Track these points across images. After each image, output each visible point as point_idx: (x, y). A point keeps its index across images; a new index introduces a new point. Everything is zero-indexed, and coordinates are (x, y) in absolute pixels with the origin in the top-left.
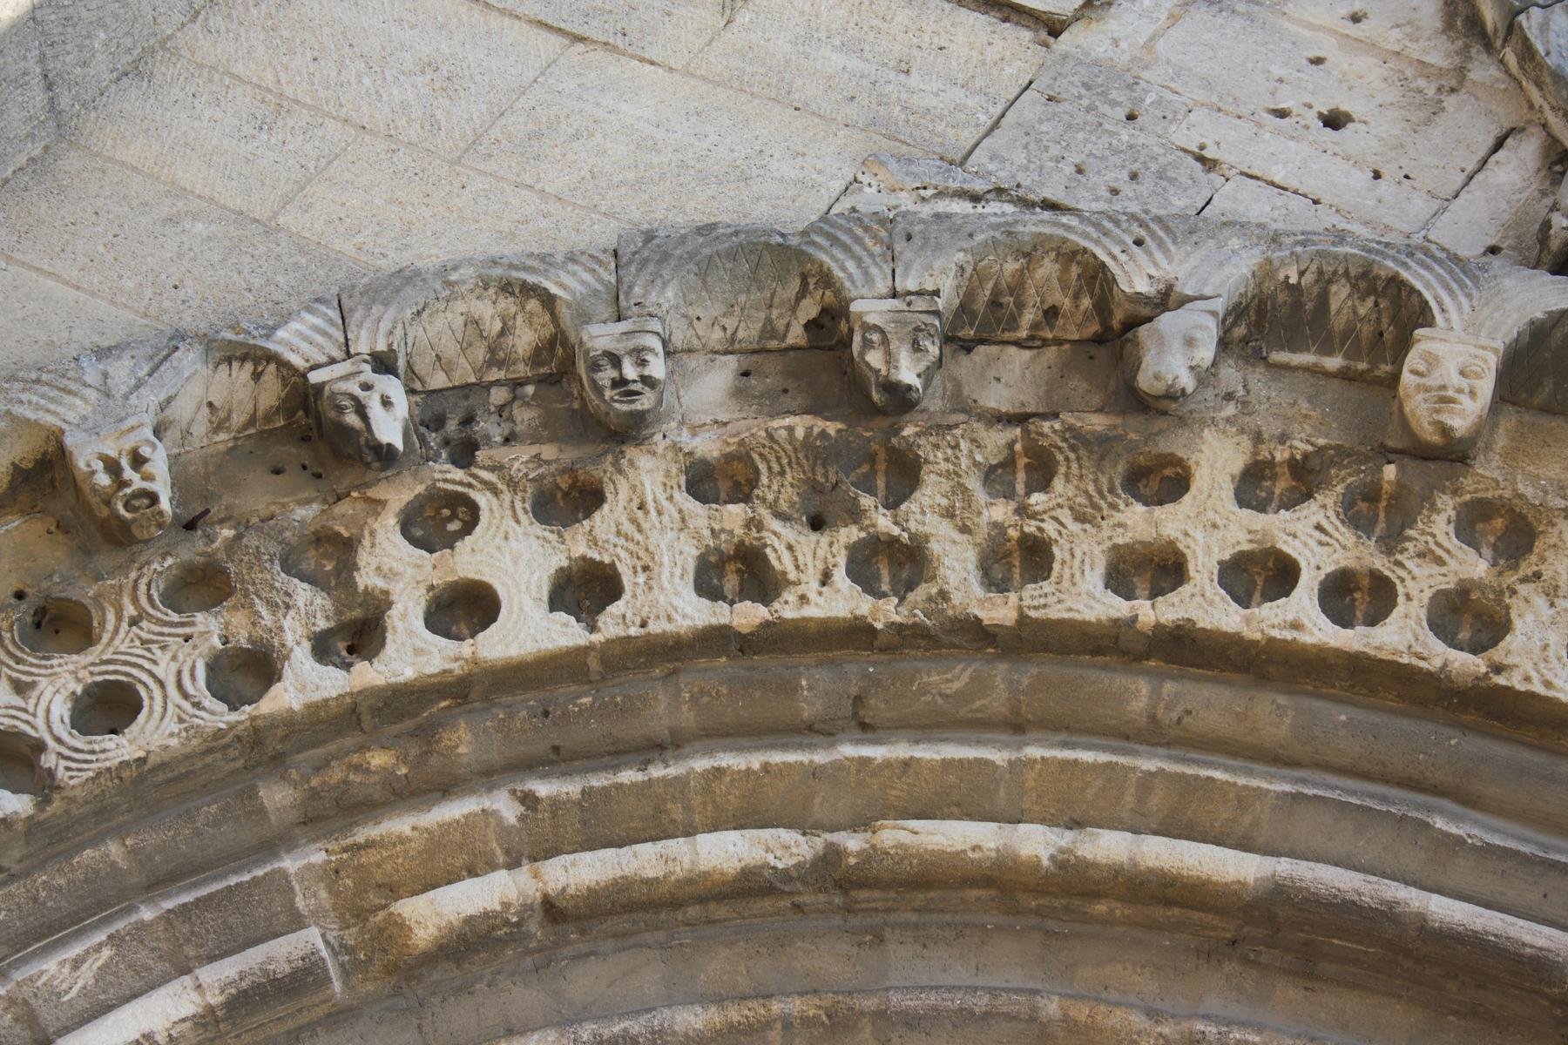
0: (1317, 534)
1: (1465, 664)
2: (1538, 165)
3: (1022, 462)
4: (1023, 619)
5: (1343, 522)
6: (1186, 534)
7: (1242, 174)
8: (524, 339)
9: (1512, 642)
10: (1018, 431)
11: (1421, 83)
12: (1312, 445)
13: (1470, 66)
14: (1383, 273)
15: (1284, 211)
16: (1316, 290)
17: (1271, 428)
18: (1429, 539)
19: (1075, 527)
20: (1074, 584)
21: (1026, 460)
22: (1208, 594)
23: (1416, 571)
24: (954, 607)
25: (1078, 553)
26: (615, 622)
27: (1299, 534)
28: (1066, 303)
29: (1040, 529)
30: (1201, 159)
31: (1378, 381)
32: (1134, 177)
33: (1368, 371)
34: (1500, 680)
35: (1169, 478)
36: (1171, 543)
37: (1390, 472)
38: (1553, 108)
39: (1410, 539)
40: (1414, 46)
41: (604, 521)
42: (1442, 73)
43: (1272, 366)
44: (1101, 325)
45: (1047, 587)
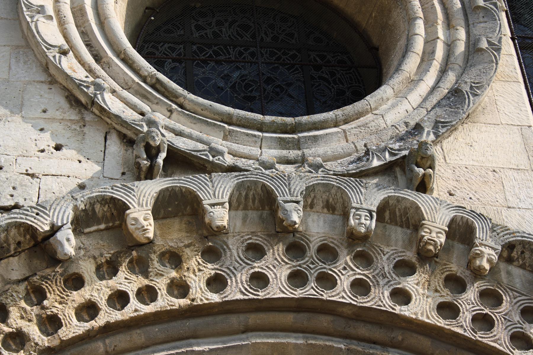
0: (126, 281)
1: (184, 302)
2: (120, 142)
3: (31, 291)
4: (62, 341)
5: (131, 274)
6: (92, 296)
7: (43, 175)
10: (26, 283)
11: (74, 127)
12: (110, 254)
13: (84, 116)
14: (108, 197)
15: (62, 183)
16: (91, 209)
17: (97, 253)
18: (156, 269)
19: (60, 306)
20: (71, 325)
21: (32, 290)
22: (108, 311)
23: (157, 280)
24: (41, 346)
25: (67, 315)
27: (122, 282)
28: (22, 239)
29: (52, 312)
30: (28, 175)
31: (116, 227)
32: (14, 188)
33: (113, 225)
34: (195, 303)
35: (74, 279)
36: (90, 300)
37: (134, 253)
38: (116, 124)
39: (151, 272)
40: (65, 115)
42: (78, 122)
43: (85, 234)
44: (34, 241)
45: (64, 328)
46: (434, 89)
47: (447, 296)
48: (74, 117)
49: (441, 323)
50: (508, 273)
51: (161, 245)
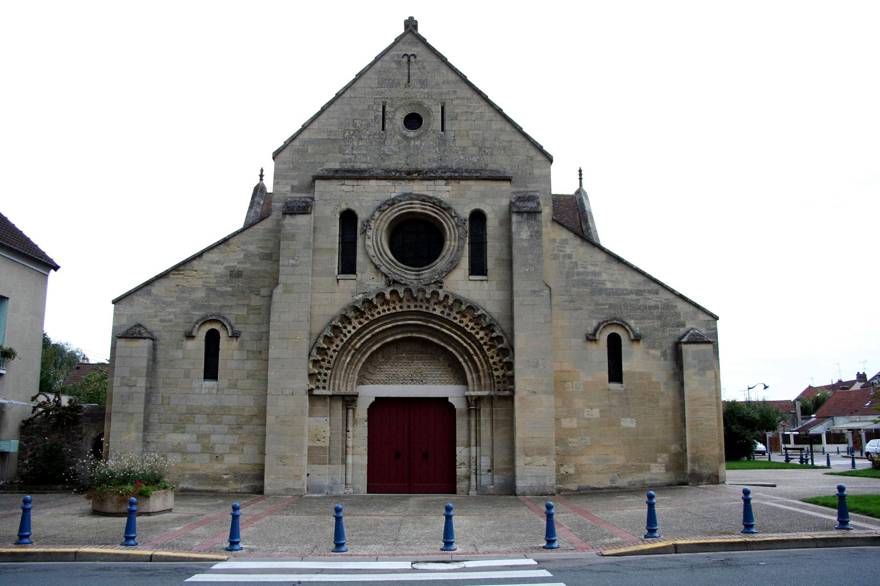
26: (357, 329)
41: (353, 323)
47: (443, 309)
49: (441, 315)
51: (392, 300)
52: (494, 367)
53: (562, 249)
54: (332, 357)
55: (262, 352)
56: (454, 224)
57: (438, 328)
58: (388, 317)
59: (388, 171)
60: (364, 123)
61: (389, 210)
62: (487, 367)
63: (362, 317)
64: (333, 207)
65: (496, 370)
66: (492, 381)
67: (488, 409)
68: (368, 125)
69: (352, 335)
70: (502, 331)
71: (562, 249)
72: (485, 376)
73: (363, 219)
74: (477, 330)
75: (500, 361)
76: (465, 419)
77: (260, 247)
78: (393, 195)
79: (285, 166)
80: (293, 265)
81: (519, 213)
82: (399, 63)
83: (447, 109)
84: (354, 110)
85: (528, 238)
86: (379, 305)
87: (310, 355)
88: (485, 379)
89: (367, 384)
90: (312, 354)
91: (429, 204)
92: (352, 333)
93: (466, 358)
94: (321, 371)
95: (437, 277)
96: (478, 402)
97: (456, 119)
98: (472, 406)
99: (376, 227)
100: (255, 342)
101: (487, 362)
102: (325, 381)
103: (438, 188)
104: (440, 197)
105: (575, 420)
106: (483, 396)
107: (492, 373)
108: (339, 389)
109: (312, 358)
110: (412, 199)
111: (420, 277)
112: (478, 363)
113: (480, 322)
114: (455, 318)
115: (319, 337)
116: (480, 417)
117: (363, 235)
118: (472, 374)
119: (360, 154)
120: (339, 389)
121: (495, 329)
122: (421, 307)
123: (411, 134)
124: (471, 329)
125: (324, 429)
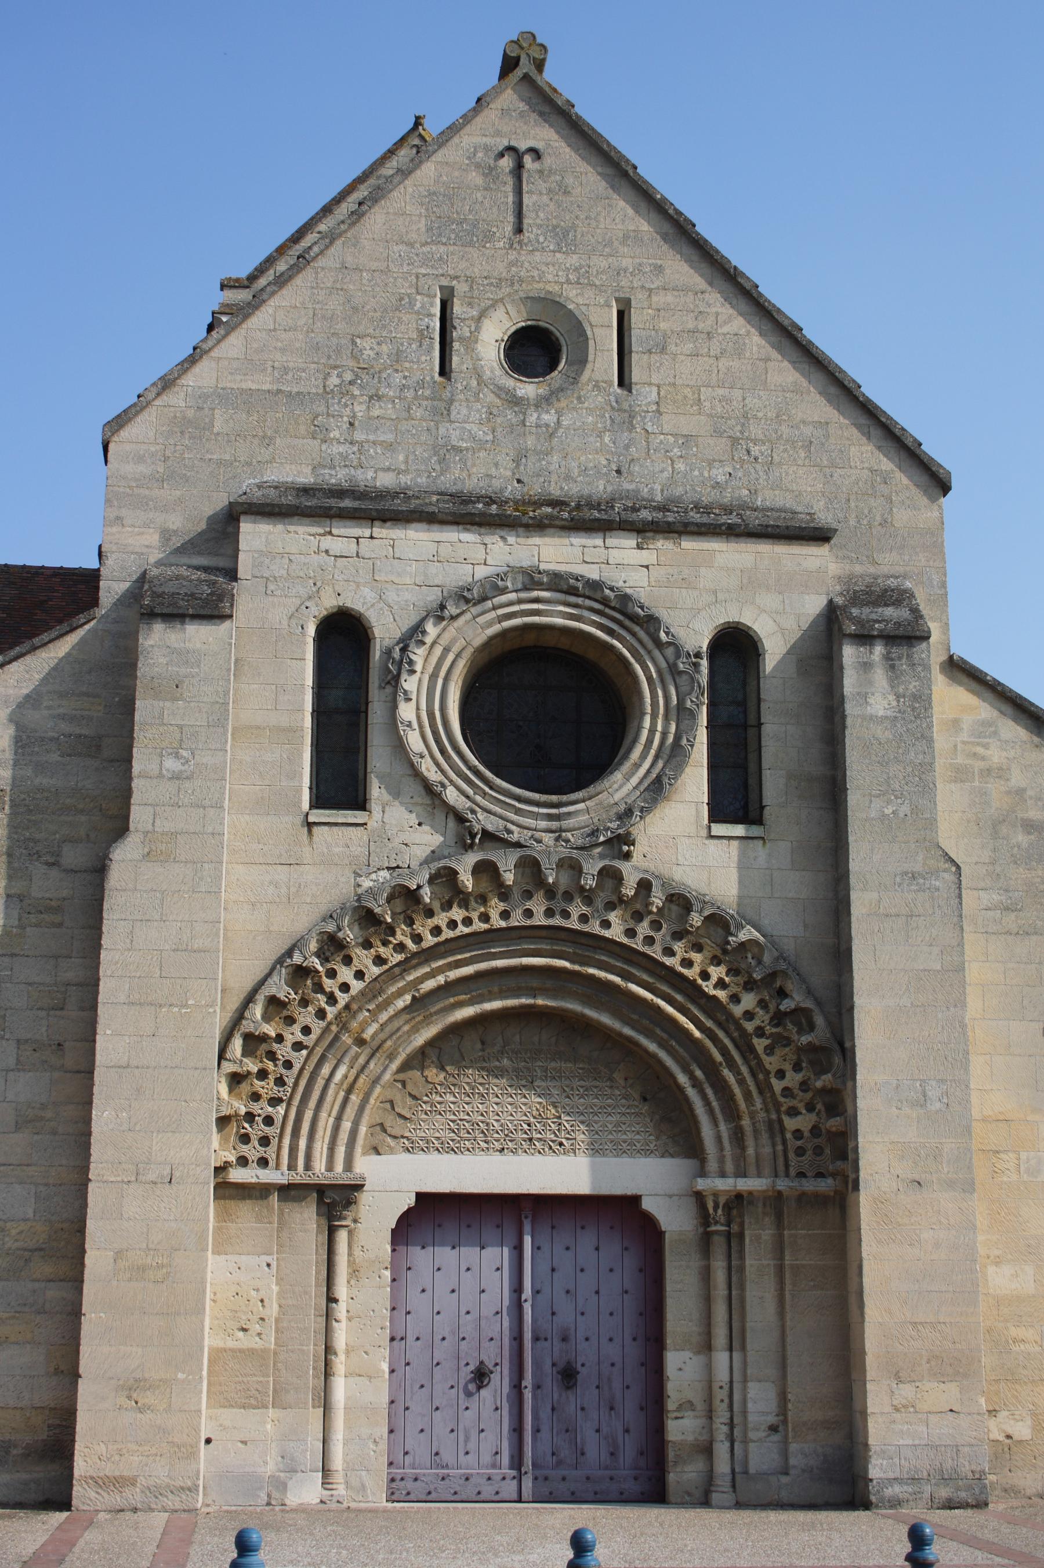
1: (485, 926)
8: (325, 937)
9: (491, 920)
41: (355, 961)
46: (649, 772)
47: (631, 924)
48: (429, 802)
49: (625, 940)
50: (669, 909)
52: (786, 1103)
53: (980, 750)
54: (288, 1065)
55: (67, 1045)
56: (663, 665)
57: (617, 980)
58: (462, 943)
59: (463, 499)
60: (384, 348)
61: (468, 616)
62: (764, 1102)
63: (385, 943)
64: (293, 602)
65: (793, 1112)
66: (780, 1148)
67: (767, 1234)
68: (398, 356)
69: (353, 998)
70: (809, 992)
71: (980, 750)
72: (756, 1131)
73: (387, 642)
74: (734, 989)
75: (804, 1086)
76: (695, 1262)
77: (62, 717)
78: (481, 572)
79: (142, 469)
80: (176, 777)
81: (864, 638)
82: (489, 172)
83: (636, 319)
84: (355, 309)
85: (889, 713)
86: (436, 906)
87: (221, 1057)
88: (756, 1139)
89: (392, 1151)
90: (228, 1055)
91: (588, 603)
92: (353, 992)
93: (699, 1073)
94: (256, 1108)
95: (613, 825)
96: (735, 1212)
97: (663, 350)
98: (716, 1223)
99: (430, 669)
100: (43, 1014)
101: (764, 1088)
102: (265, 1141)
103: (615, 556)
104: (621, 584)
105: (1029, 1270)
106: (750, 1193)
107: (780, 1121)
108: (308, 1167)
109: (229, 1067)
110: (538, 585)
111: (565, 824)
112: (737, 1091)
113: (743, 966)
114: (669, 952)
115: (249, 999)
116: (742, 1257)
117: (389, 689)
118: (716, 1124)
119: (374, 443)
120: (308, 1167)
121: (789, 986)
122: (566, 915)
123: (528, 389)
124: (715, 987)
125: (262, 1294)
